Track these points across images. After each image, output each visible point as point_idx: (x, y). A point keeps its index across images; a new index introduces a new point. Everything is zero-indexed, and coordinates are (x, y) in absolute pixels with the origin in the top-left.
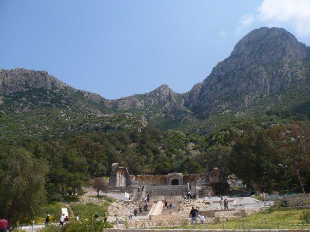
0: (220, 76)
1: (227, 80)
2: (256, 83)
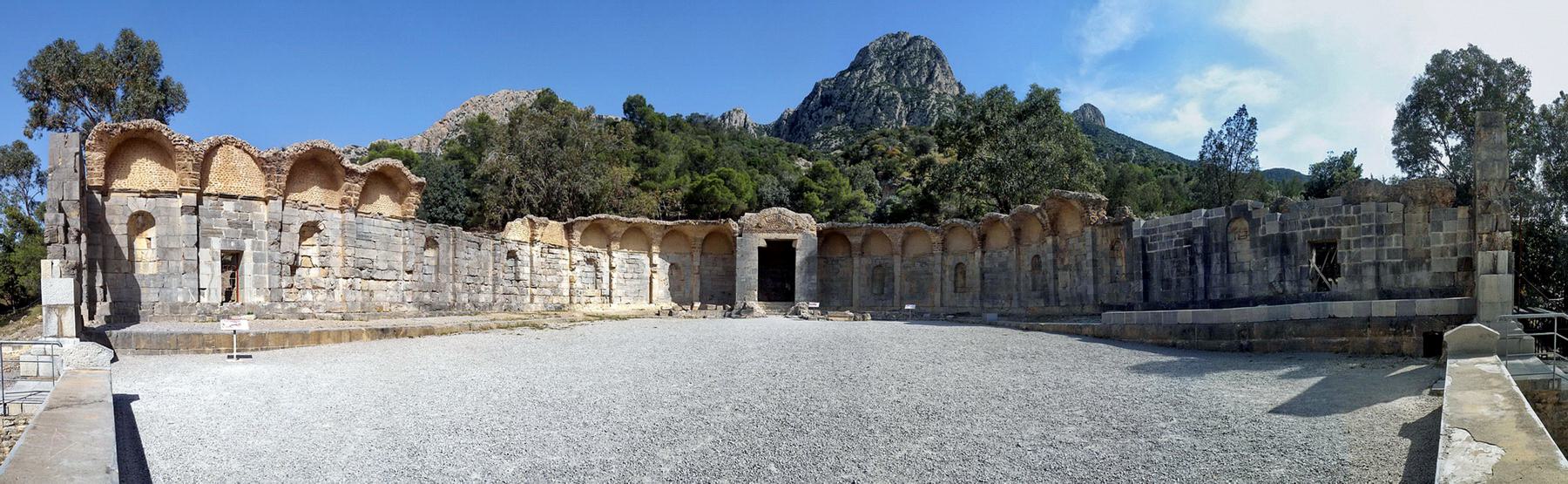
1: (842, 104)
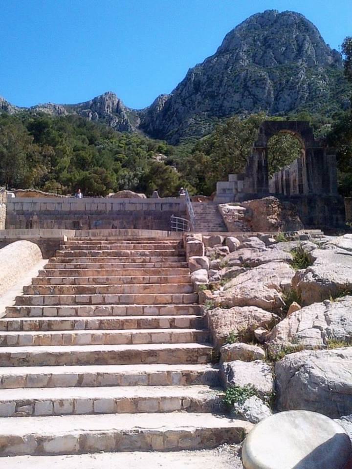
0: (199, 82)
2: (254, 95)
